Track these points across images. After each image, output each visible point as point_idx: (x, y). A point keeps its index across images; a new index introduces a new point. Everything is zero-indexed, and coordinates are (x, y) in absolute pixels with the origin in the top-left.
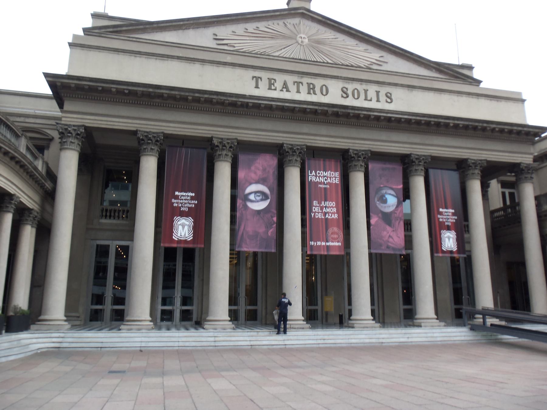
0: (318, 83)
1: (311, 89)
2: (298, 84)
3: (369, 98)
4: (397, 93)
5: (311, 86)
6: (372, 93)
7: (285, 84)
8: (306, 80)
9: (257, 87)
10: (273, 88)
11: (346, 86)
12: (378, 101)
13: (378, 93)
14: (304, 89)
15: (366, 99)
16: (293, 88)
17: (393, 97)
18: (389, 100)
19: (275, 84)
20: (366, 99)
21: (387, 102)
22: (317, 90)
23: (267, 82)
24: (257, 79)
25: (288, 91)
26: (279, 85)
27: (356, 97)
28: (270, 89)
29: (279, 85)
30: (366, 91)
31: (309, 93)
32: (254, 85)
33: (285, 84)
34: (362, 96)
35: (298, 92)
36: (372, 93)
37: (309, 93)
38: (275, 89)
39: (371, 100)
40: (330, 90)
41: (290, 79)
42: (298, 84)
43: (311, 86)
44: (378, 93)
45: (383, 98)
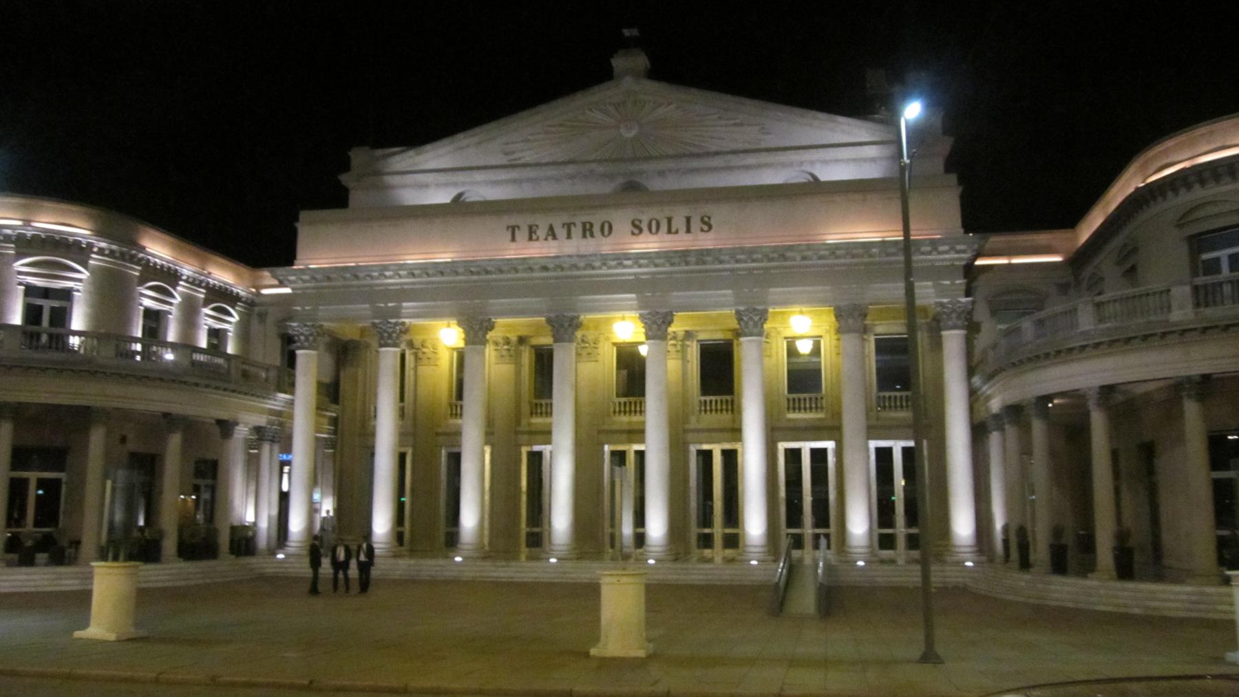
0: (597, 219)
1: (587, 230)
2: (568, 227)
3: (674, 230)
4: (719, 213)
5: (588, 226)
6: (679, 223)
7: (551, 229)
8: (580, 219)
9: (513, 239)
10: (534, 237)
11: (641, 217)
12: (688, 231)
13: (688, 220)
14: (577, 231)
15: (669, 231)
16: (561, 232)
17: (712, 222)
18: (706, 228)
19: (539, 233)
20: (669, 231)
21: (702, 230)
22: (596, 229)
23: (527, 232)
24: (513, 229)
25: (555, 238)
26: (541, 232)
27: (654, 229)
28: (531, 239)
29: (541, 232)
30: (669, 220)
31: (584, 236)
32: (510, 237)
33: (551, 229)
34: (664, 227)
35: (569, 236)
36: (679, 223)
37: (584, 236)
38: (538, 239)
39: (677, 232)
40: (614, 227)
41: (558, 221)
42: (568, 227)
43: (588, 226)
44: (688, 220)
45: (696, 224)
